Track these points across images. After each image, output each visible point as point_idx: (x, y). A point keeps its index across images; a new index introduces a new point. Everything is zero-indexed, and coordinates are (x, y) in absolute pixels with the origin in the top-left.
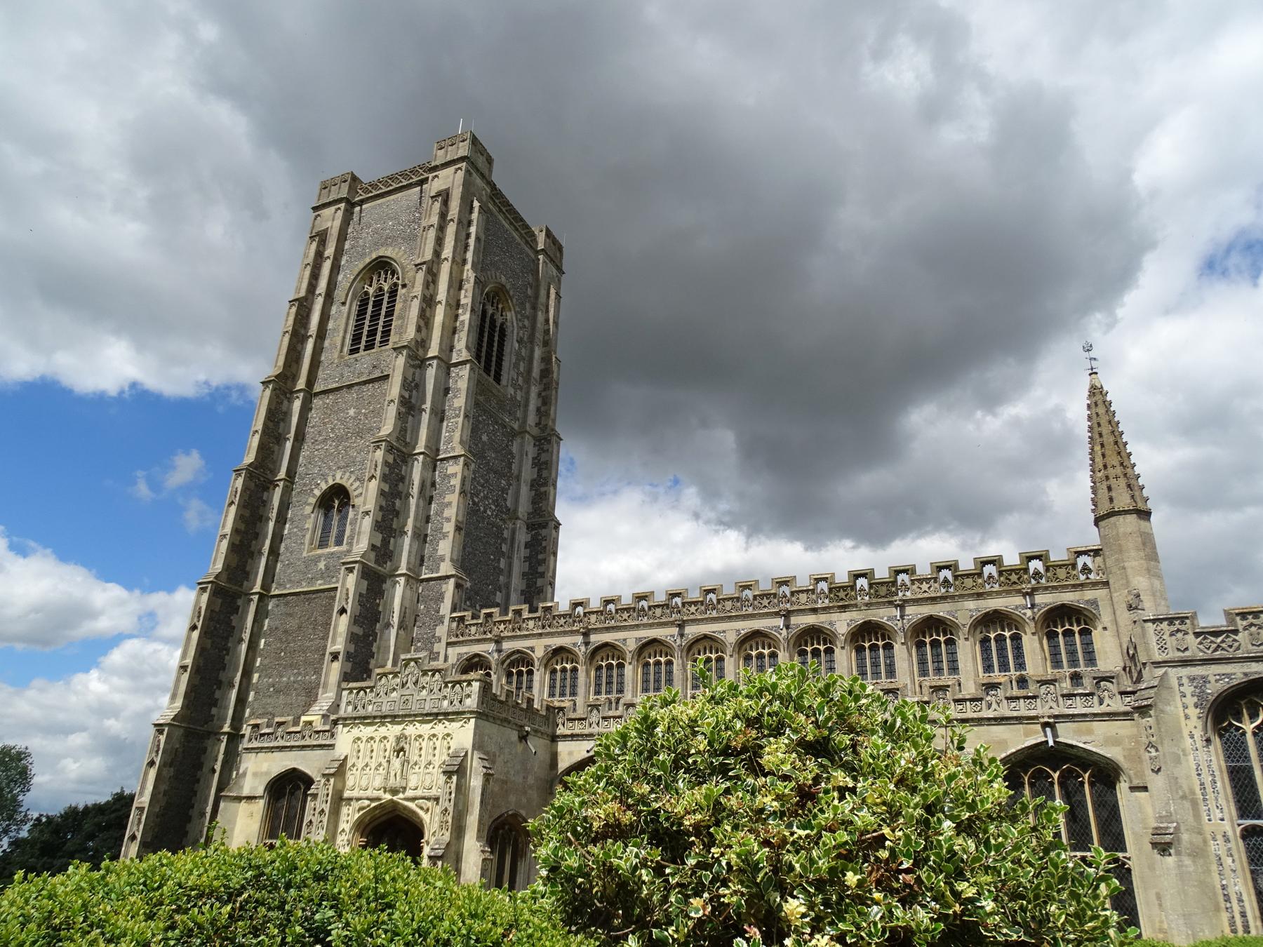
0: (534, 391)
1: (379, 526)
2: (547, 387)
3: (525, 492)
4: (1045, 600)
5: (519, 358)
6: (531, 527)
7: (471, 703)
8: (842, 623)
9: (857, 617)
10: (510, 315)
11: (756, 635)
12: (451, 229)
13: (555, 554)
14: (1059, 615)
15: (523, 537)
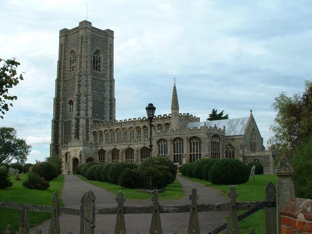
0: (108, 70)
1: (77, 110)
2: (111, 69)
3: (108, 93)
4: (165, 122)
5: (104, 63)
6: (110, 100)
7: (82, 144)
8: (141, 126)
9: (143, 125)
10: (101, 55)
11: (131, 127)
12: (83, 45)
13: (115, 106)
14: (167, 124)
15: (108, 102)
